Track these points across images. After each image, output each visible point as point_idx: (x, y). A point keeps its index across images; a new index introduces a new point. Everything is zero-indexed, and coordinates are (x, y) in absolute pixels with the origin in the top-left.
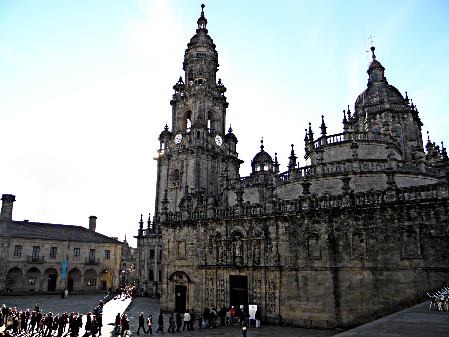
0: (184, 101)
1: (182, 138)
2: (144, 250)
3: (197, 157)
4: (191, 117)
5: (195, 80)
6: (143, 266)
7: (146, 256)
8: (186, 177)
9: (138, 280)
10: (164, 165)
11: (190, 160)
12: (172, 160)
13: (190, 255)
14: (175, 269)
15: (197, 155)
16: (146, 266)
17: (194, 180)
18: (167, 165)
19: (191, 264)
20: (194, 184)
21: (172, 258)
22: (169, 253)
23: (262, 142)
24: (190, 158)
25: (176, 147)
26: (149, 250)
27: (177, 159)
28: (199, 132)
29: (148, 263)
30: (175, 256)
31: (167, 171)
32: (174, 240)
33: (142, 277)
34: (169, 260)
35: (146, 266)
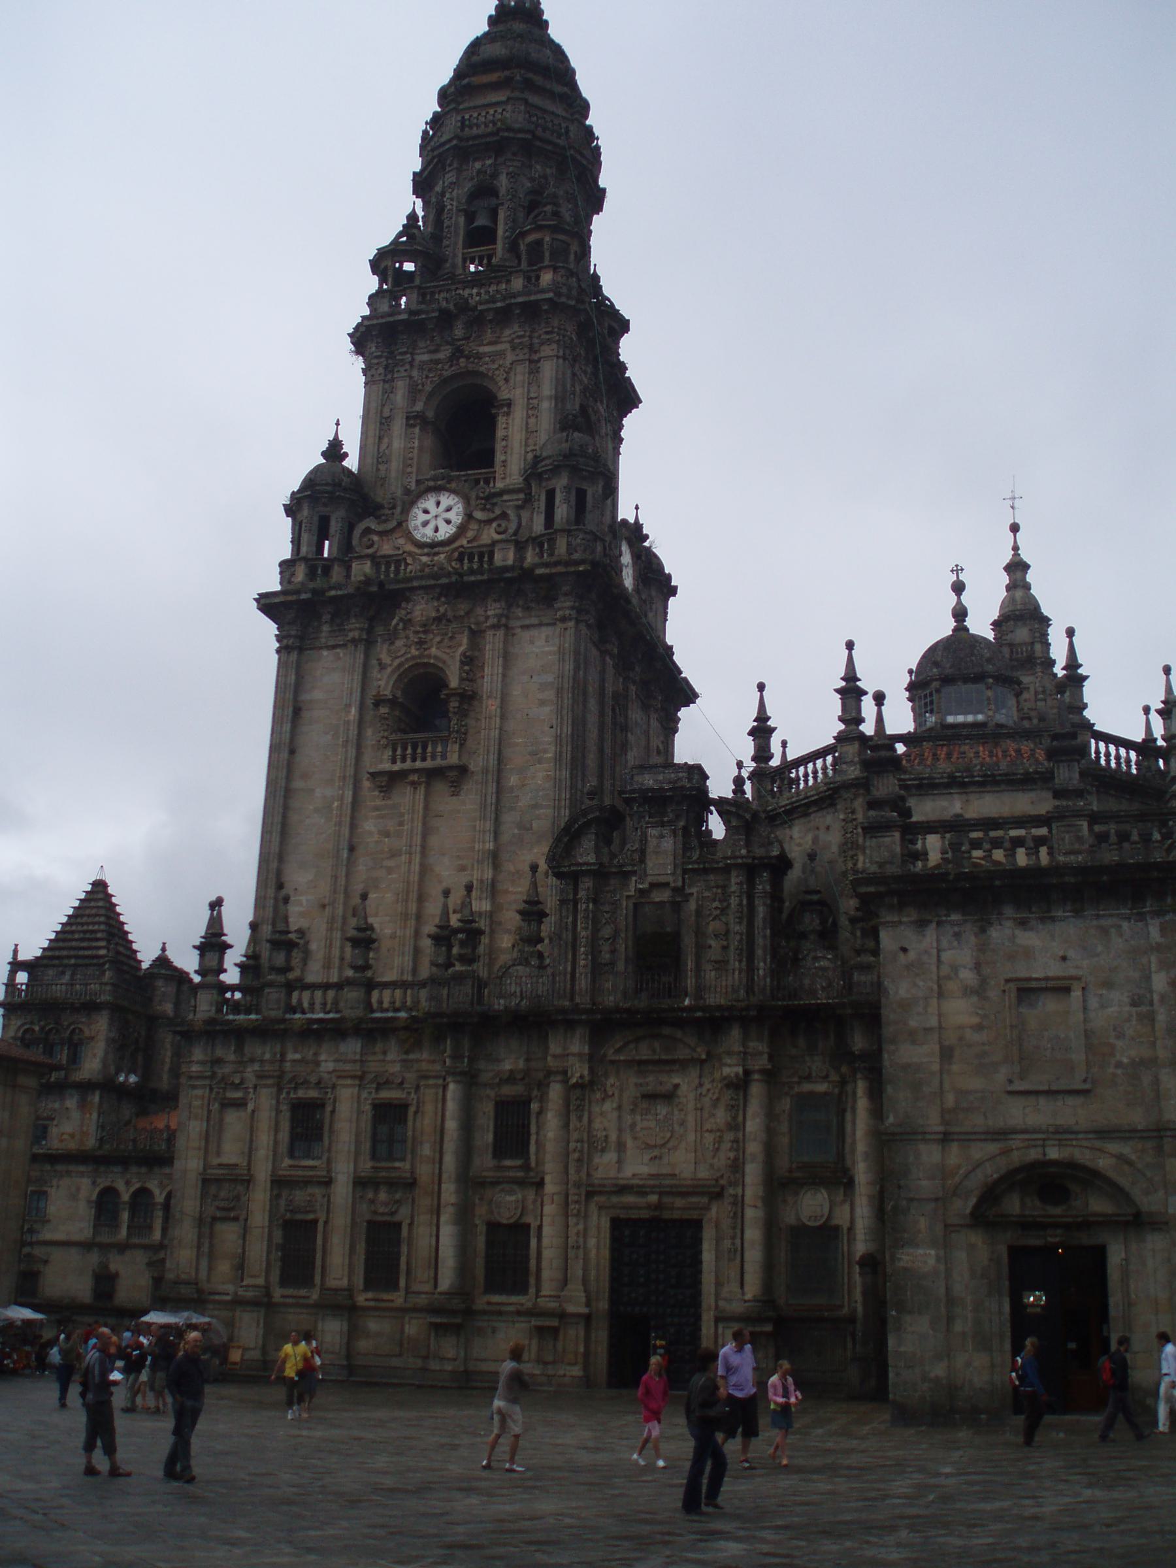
0: (459, 332)
1: (469, 516)
2: (240, 1104)
3: (578, 621)
4: (501, 421)
5: (531, 238)
6: (237, 1198)
7: (264, 1139)
8: (503, 717)
9: (197, 1284)
10: (334, 647)
11: (526, 635)
12: (407, 623)
13: (1119, 1065)
14: (1006, 1152)
15: (579, 611)
16: (259, 1199)
17: (558, 739)
18: (361, 648)
19: (1137, 1118)
20: (558, 759)
21: (976, 1083)
22: (946, 1054)
23: (958, 588)
24: (527, 622)
25: (424, 559)
26: (284, 1107)
27: (438, 620)
28: (581, 495)
29: (279, 1183)
30: (1002, 1075)
31: (358, 677)
32: (983, 982)
33: (224, 1267)
34: (950, 1100)
35: (259, 1199)
